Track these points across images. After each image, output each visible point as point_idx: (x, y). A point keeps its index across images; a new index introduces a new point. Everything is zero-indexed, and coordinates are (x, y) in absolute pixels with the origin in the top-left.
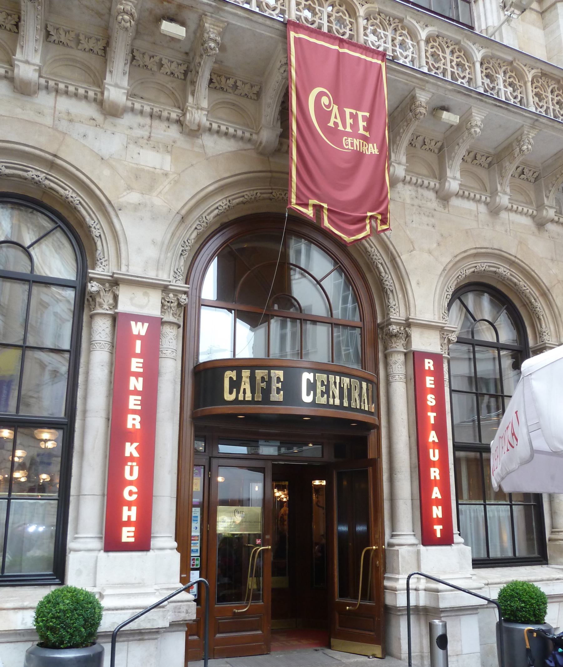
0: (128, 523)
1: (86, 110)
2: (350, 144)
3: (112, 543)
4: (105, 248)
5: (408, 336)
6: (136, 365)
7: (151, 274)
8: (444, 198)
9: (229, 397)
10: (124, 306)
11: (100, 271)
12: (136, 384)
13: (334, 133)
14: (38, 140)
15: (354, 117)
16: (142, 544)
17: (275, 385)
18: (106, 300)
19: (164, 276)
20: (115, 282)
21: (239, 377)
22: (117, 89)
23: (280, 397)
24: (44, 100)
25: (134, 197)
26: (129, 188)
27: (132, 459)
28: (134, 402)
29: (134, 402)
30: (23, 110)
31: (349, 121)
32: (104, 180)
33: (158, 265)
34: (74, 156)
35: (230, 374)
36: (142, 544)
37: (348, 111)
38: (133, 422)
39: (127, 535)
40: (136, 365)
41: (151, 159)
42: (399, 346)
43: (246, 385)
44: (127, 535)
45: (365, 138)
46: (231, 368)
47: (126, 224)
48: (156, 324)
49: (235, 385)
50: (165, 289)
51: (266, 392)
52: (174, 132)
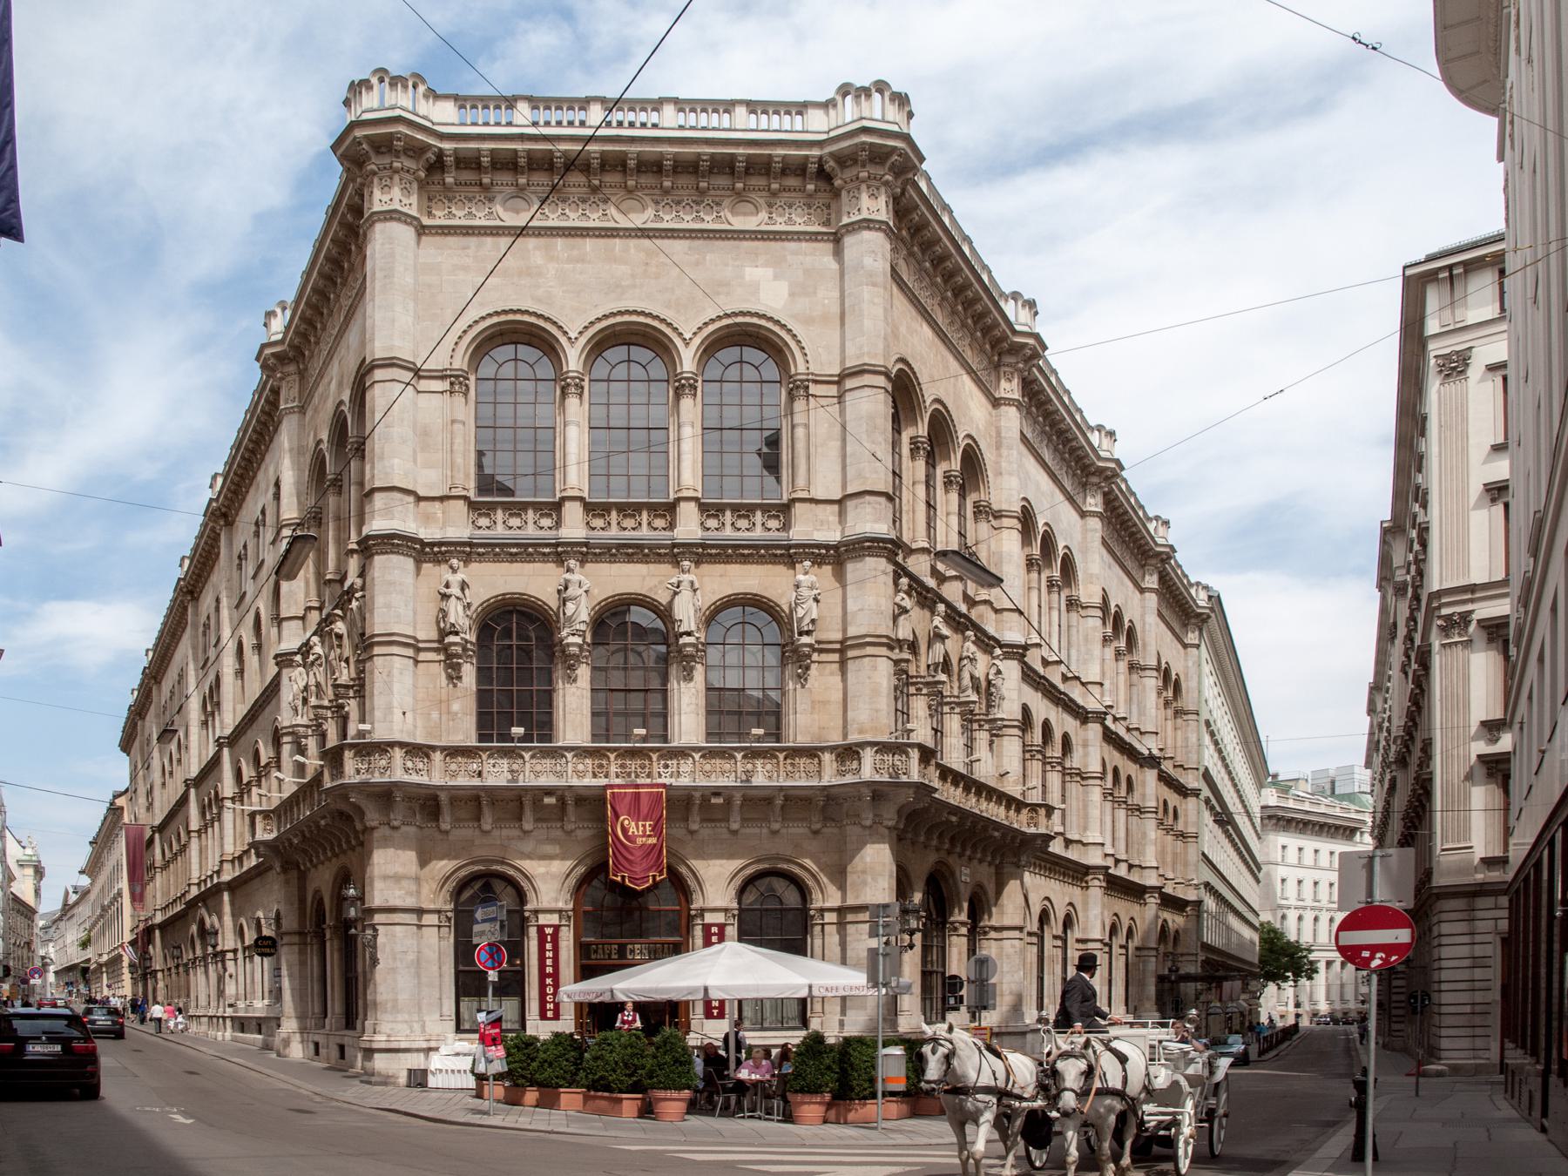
1: (516, 833)
3: (543, 1016)
4: (531, 895)
6: (549, 946)
7: (553, 906)
10: (541, 922)
16: (556, 1017)
19: (561, 905)
20: (536, 912)
22: (527, 826)
28: (549, 962)
29: (549, 962)
36: (556, 1017)
38: (549, 970)
39: (550, 1014)
40: (549, 946)
44: (550, 1014)
47: (539, 884)
48: (557, 928)
52: (559, 833)
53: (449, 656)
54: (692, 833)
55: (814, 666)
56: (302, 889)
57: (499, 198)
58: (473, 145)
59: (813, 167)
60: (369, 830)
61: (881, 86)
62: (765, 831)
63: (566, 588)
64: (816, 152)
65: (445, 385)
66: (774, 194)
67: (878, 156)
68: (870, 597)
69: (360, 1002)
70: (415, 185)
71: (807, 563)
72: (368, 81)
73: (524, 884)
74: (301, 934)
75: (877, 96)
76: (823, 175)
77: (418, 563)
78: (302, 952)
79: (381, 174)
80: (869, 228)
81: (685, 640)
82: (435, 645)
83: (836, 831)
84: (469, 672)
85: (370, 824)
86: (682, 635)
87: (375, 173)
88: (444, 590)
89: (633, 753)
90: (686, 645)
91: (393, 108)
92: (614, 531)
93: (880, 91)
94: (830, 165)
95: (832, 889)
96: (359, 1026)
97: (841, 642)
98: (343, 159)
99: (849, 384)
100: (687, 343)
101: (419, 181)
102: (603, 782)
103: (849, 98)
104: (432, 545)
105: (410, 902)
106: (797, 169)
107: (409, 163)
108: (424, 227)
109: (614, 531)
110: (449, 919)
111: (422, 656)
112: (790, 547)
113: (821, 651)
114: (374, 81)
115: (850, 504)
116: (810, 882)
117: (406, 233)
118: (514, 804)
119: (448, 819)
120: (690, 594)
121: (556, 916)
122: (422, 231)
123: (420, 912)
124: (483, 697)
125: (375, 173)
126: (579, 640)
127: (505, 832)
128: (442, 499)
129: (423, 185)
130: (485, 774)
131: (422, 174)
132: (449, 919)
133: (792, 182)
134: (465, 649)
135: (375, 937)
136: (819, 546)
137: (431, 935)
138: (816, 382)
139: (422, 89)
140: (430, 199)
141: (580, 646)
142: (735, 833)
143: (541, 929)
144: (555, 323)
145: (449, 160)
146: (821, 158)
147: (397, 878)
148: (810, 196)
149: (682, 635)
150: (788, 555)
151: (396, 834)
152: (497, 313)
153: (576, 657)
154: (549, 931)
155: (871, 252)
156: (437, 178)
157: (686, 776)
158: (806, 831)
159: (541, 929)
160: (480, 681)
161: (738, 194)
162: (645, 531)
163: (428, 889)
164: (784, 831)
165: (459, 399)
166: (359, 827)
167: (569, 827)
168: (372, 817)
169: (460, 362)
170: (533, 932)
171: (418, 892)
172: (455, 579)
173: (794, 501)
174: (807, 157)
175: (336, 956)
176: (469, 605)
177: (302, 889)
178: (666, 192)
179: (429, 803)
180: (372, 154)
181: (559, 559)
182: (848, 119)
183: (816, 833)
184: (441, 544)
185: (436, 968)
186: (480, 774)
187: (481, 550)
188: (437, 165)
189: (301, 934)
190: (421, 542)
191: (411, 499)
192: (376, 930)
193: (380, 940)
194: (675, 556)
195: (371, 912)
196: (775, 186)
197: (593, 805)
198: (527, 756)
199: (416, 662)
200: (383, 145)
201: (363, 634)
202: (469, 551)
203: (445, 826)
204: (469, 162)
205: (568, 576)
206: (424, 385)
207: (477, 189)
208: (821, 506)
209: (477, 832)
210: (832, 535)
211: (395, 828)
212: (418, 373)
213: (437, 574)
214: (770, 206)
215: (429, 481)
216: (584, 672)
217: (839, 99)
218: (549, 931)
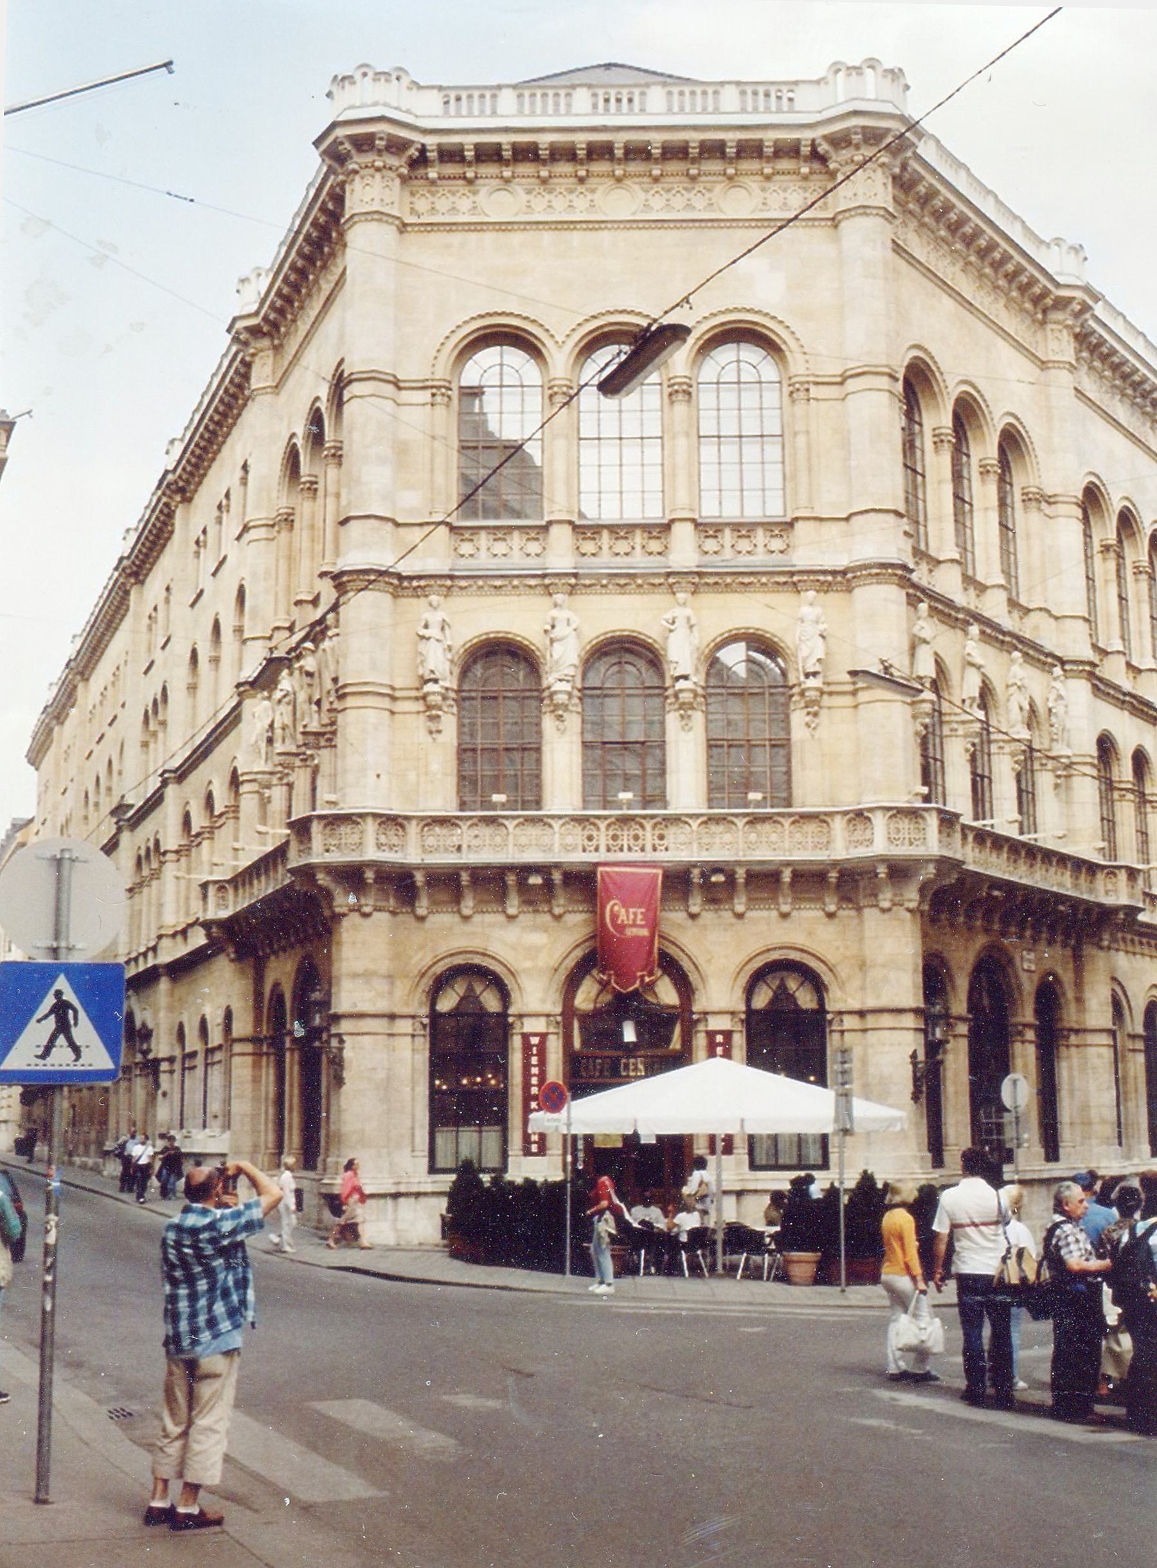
1: (501, 918)
3: (527, 1152)
4: (515, 995)
6: (534, 1060)
10: (526, 1030)
12: (535, 1070)
14: (476, 944)
18: (517, 1025)
20: (521, 1016)
24: (477, 918)
25: (528, 964)
30: (467, 928)
33: (543, 1001)
34: (495, 948)
39: (534, 1148)
40: (534, 1060)
41: (538, 939)
47: (524, 981)
48: (543, 1037)
53: (429, 707)
54: (693, 916)
55: (824, 713)
56: (259, 980)
57: (483, 191)
58: (455, 139)
59: (805, 150)
60: (337, 918)
61: (872, 63)
62: (774, 913)
63: (553, 627)
65: (425, 396)
66: (768, 178)
67: (872, 136)
68: (878, 625)
69: (323, 1133)
70: (398, 181)
71: (812, 593)
72: (351, 77)
74: (255, 1040)
75: (869, 72)
76: (816, 156)
77: (395, 596)
78: (256, 1066)
79: (362, 172)
81: (682, 684)
82: (414, 693)
83: (853, 913)
84: (449, 723)
85: (337, 910)
86: (678, 679)
87: (356, 172)
88: (423, 632)
89: (625, 820)
90: (681, 691)
91: (375, 104)
92: (605, 558)
93: (872, 67)
94: (824, 147)
96: (320, 1165)
98: (326, 153)
99: (851, 385)
101: (400, 176)
102: (592, 857)
103: (841, 74)
104: (411, 578)
105: (382, 1006)
106: (791, 150)
107: (393, 161)
108: (405, 225)
109: (607, 556)
110: (424, 1026)
111: (400, 706)
112: (792, 574)
113: (831, 694)
114: (358, 76)
115: (854, 519)
117: (389, 232)
118: (493, 883)
120: (686, 630)
121: (543, 1020)
122: (403, 227)
123: (392, 1017)
124: (464, 752)
125: (356, 172)
126: (567, 687)
127: (488, 918)
129: (405, 180)
130: (464, 848)
131: (404, 171)
132: (424, 1026)
133: (785, 164)
134: (445, 698)
135: (341, 1050)
136: (824, 572)
137: (404, 1045)
139: (405, 81)
140: (412, 194)
141: (570, 695)
142: (740, 916)
143: (525, 1037)
145: (432, 155)
146: (813, 141)
147: (367, 975)
148: (805, 178)
149: (678, 679)
150: (793, 581)
151: (368, 922)
152: (481, 316)
153: (566, 707)
154: (535, 1040)
155: (867, 239)
156: (421, 172)
157: (684, 848)
158: (821, 914)
159: (525, 1037)
160: (460, 734)
161: (730, 178)
162: (638, 557)
163: (402, 988)
164: (794, 913)
165: (440, 411)
166: (327, 913)
167: (557, 911)
168: (344, 900)
169: (442, 371)
170: (516, 1042)
171: (391, 993)
172: (435, 618)
173: (797, 519)
174: (799, 140)
175: (296, 1068)
176: (450, 648)
177: (259, 980)
178: (656, 180)
179: (400, 885)
180: (353, 152)
181: (548, 591)
182: (841, 99)
183: (831, 916)
184: (420, 577)
185: (408, 1089)
186: (459, 848)
187: (463, 583)
188: (421, 160)
189: (255, 1040)
190: (400, 577)
191: (390, 524)
192: (342, 1041)
193: (347, 1054)
194: (671, 586)
195: (337, 1018)
196: (768, 170)
197: (583, 883)
198: (510, 825)
199: (392, 713)
200: (364, 143)
201: (335, 680)
202: (449, 582)
203: (421, 912)
204: (452, 155)
205: (555, 613)
206: (406, 396)
207: (461, 182)
209: (457, 918)
210: (841, 561)
211: (366, 915)
212: (397, 384)
213: (417, 609)
214: (763, 190)
215: (410, 503)
216: (573, 721)
217: (830, 77)
218: (535, 1040)
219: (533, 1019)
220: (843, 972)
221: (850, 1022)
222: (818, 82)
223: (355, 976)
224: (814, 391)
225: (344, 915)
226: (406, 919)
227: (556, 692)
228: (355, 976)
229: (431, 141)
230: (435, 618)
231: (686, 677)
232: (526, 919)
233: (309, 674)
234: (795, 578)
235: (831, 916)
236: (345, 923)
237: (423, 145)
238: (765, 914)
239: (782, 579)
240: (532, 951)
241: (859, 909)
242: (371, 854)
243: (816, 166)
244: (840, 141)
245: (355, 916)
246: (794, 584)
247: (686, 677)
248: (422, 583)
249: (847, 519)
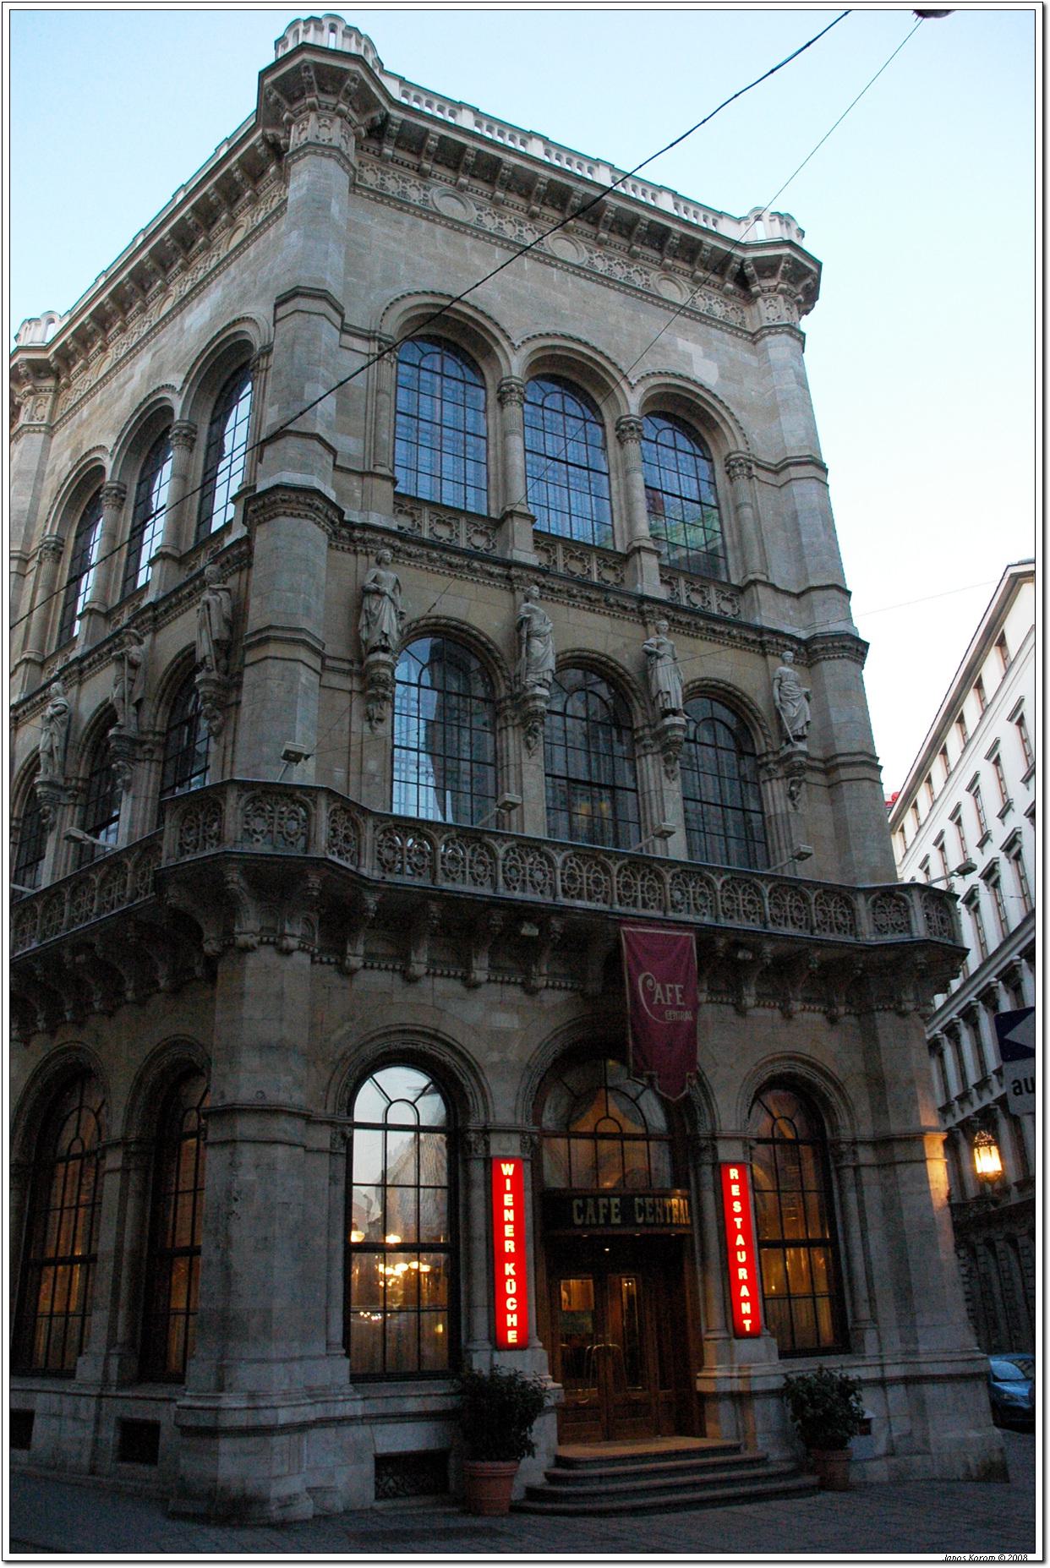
0: (512, 1328)
1: (456, 986)
2: (671, 1015)
4: (475, 1101)
5: (715, 1148)
8: (741, 1011)
9: (578, 1221)
11: (475, 1123)
13: (660, 1010)
14: (427, 1020)
15: (672, 990)
17: (614, 1211)
21: (585, 1205)
23: (617, 1221)
25: (495, 1057)
26: (491, 1049)
27: (510, 1276)
31: (669, 995)
32: (473, 1046)
34: (449, 1029)
35: (577, 1202)
37: (668, 986)
39: (512, 1337)
41: (505, 1021)
42: (707, 1157)
43: (590, 1211)
45: (680, 1008)
46: (578, 1197)
47: (489, 1079)
49: (582, 1211)
50: (522, 1133)
51: (607, 1217)
59: (734, 266)
64: (738, 253)
73: (468, 1083)
80: (791, 334)
82: (346, 666)
94: (749, 270)
95: (863, 1107)
97: (825, 761)
99: (794, 472)
100: (632, 387)
101: (357, 135)
104: (352, 526)
116: (835, 1099)
119: (361, 949)
127: (440, 984)
128: (362, 474)
138: (758, 466)
144: (497, 324)
154: (508, 1169)
188: (378, 131)
208: (781, 596)
219: (504, 1137)
220: (851, 1092)
221: (865, 1155)
222: (739, 221)
223: (265, 1048)
224: (755, 471)
225: (247, 949)
226: (330, 974)
227: (535, 697)
228: (265, 1048)
229: (394, 112)
230: (388, 575)
231: (674, 712)
232: (492, 992)
233: (134, 666)
234: (766, 638)
235: (833, 1020)
236: (251, 961)
237: (388, 115)
238: (768, 1012)
239: (752, 636)
240: (500, 1038)
241: (864, 1013)
242: (320, 849)
243: (738, 290)
244: (767, 267)
245: (266, 955)
246: (762, 644)
247: (674, 712)
248: (368, 535)
249: (798, 596)
